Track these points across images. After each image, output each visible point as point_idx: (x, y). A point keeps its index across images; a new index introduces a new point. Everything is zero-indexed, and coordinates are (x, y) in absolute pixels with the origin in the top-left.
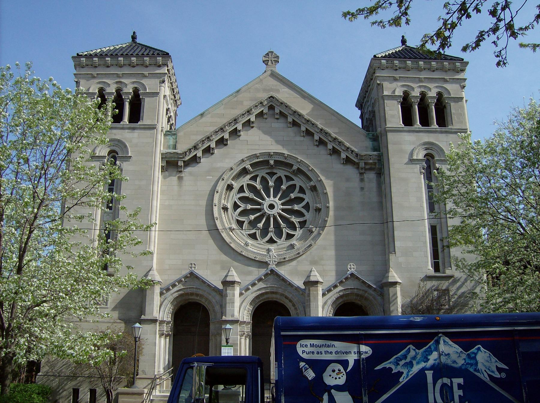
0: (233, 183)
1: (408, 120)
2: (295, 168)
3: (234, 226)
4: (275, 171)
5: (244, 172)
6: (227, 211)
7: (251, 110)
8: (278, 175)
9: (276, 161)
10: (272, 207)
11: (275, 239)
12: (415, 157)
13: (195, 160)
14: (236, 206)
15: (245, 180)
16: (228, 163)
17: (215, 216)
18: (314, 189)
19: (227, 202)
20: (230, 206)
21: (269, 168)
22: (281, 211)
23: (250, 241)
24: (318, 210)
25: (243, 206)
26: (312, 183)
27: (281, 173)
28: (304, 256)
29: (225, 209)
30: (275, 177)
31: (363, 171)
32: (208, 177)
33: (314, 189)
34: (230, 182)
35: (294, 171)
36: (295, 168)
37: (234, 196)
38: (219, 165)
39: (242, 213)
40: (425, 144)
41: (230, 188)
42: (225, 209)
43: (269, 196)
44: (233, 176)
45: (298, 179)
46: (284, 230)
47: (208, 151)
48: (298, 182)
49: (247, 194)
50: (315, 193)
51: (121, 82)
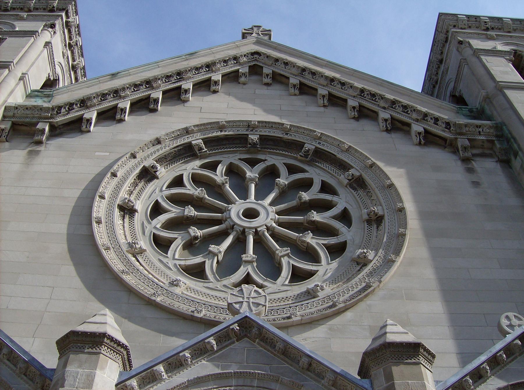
0: (158, 165)
4: (261, 157)
9: (263, 138)
10: (251, 214)
13: (77, 126)
14: (157, 210)
15: (190, 168)
17: (94, 215)
20: (142, 206)
21: (248, 152)
22: (274, 225)
24: (376, 220)
25: (174, 211)
28: (349, 315)
29: (128, 210)
30: (260, 167)
31: (468, 154)
32: (97, 154)
37: (157, 190)
38: (129, 137)
39: (170, 225)
43: (244, 196)
44: (157, 154)
46: (284, 261)
47: (110, 116)
48: (317, 174)
49: (190, 189)
50: (361, 192)
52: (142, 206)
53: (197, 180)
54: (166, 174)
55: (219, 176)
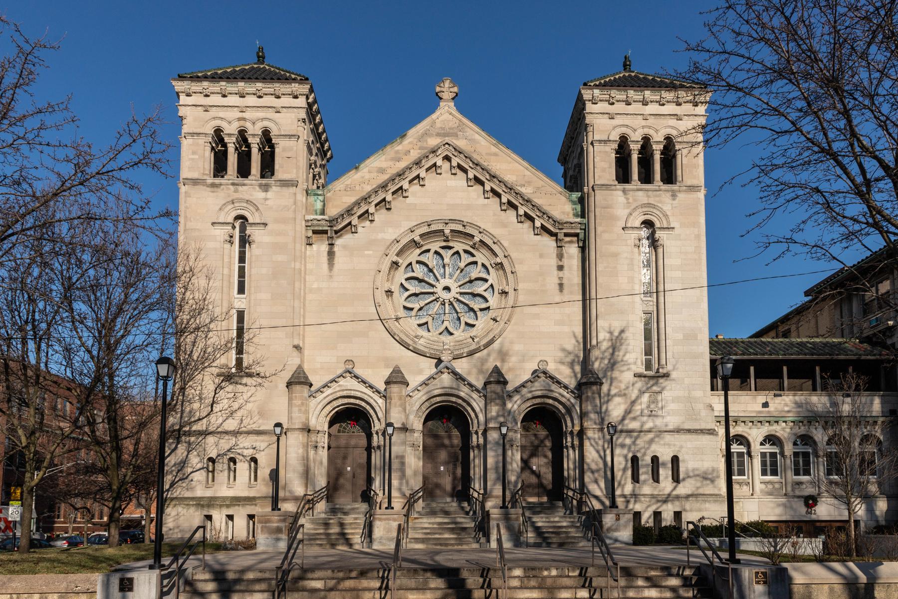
1: (623, 176)
2: (477, 239)
3: (402, 313)
4: (451, 244)
5: (415, 244)
6: (392, 295)
7: (421, 161)
8: (454, 250)
9: (452, 231)
10: (447, 289)
11: (451, 330)
12: (629, 225)
16: (391, 234)
18: (500, 266)
19: (392, 284)
20: (395, 288)
21: (445, 241)
23: (422, 332)
26: (498, 260)
27: (459, 246)
32: (366, 252)
33: (500, 266)
34: (395, 259)
35: (475, 244)
36: (477, 239)
37: (401, 276)
38: (380, 236)
40: (643, 205)
41: (395, 264)
42: (389, 293)
45: (480, 254)
48: (481, 257)
51: (244, 119)
52: (395, 288)
53: (418, 262)
54: (403, 262)
55: (431, 260)
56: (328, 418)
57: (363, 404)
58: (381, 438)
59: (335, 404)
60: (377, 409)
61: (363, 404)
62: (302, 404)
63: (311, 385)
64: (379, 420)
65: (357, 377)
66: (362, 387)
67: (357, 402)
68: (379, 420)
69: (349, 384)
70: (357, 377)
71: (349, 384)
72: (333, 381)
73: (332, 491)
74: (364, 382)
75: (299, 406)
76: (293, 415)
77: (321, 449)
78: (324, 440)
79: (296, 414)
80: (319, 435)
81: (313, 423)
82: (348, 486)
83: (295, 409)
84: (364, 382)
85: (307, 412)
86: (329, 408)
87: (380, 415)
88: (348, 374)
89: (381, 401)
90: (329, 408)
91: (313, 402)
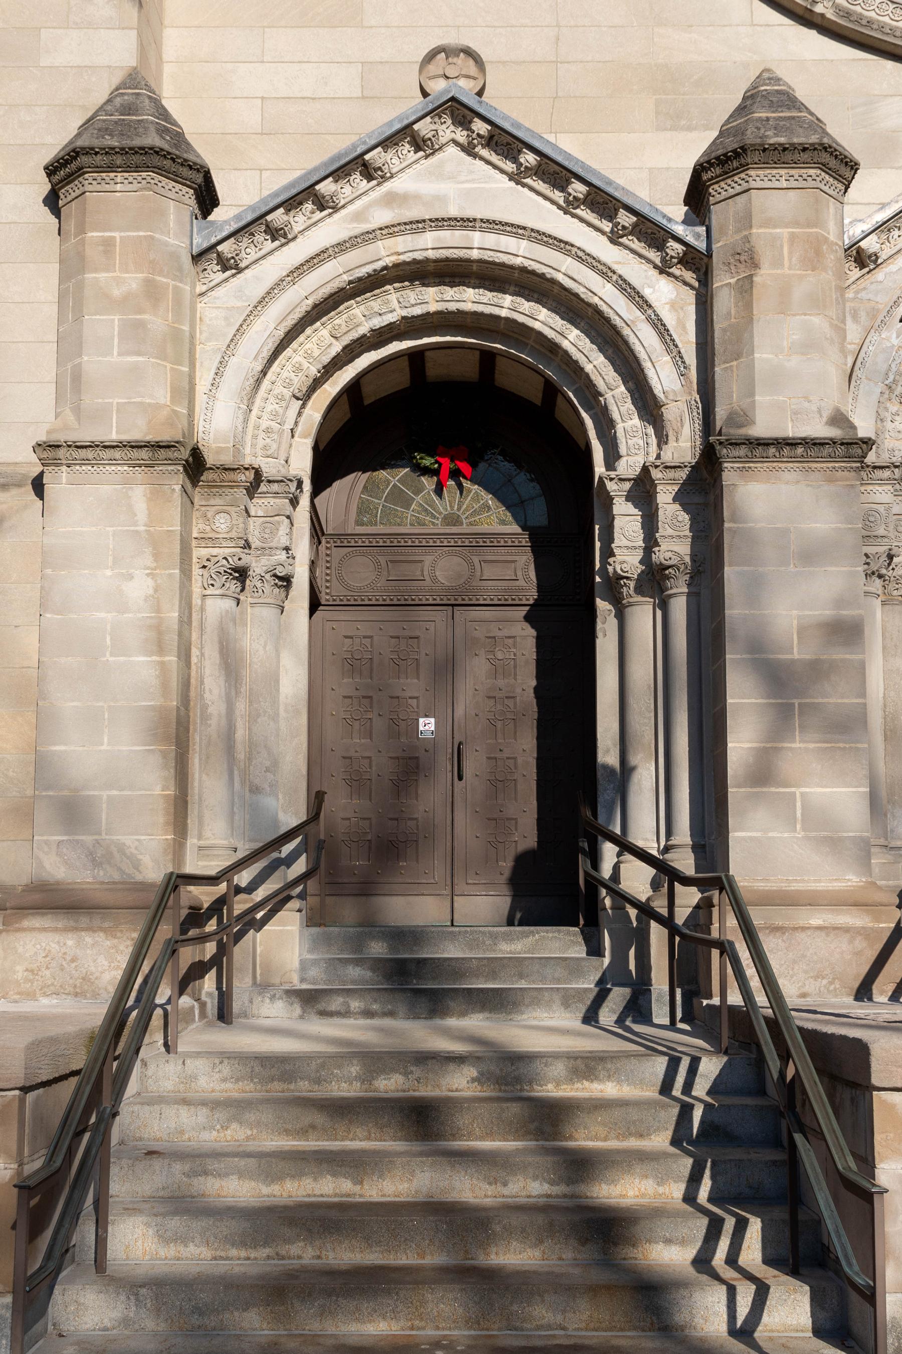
56: (315, 412)
57: (542, 319)
58: (673, 519)
59: (363, 316)
60: (644, 341)
61: (542, 319)
62: (152, 292)
63: (207, 199)
64: (649, 407)
65: (504, 143)
66: (535, 208)
67: (506, 305)
68: (649, 407)
69: (457, 192)
70: (504, 143)
71: (457, 186)
72: (358, 166)
73: (348, 853)
74: (554, 173)
75: (124, 303)
76: (93, 362)
77: (270, 592)
78: (287, 539)
79: (107, 354)
80: (260, 506)
81: (217, 425)
82: (467, 830)
83: (102, 325)
84: (554, 173)
85: (182, 348)
86: (322, 343)
87: (666, 378)
88: (447, 131)
89: (670, 297)
90: (322, 343)
91: (223, 300)
